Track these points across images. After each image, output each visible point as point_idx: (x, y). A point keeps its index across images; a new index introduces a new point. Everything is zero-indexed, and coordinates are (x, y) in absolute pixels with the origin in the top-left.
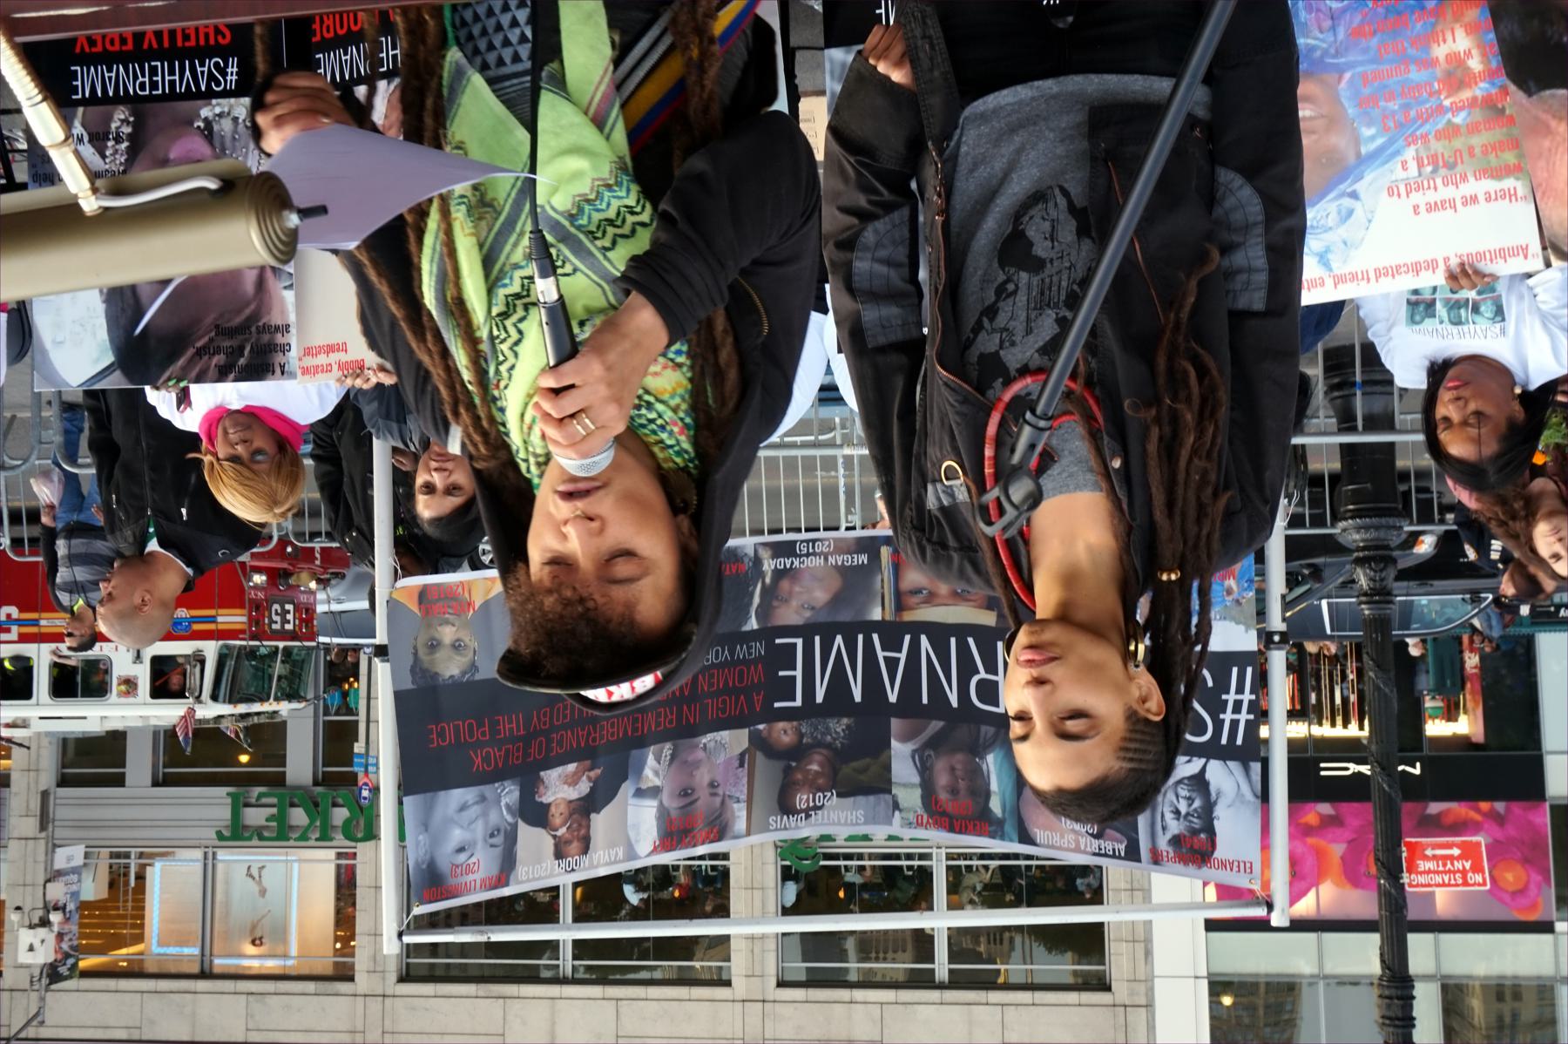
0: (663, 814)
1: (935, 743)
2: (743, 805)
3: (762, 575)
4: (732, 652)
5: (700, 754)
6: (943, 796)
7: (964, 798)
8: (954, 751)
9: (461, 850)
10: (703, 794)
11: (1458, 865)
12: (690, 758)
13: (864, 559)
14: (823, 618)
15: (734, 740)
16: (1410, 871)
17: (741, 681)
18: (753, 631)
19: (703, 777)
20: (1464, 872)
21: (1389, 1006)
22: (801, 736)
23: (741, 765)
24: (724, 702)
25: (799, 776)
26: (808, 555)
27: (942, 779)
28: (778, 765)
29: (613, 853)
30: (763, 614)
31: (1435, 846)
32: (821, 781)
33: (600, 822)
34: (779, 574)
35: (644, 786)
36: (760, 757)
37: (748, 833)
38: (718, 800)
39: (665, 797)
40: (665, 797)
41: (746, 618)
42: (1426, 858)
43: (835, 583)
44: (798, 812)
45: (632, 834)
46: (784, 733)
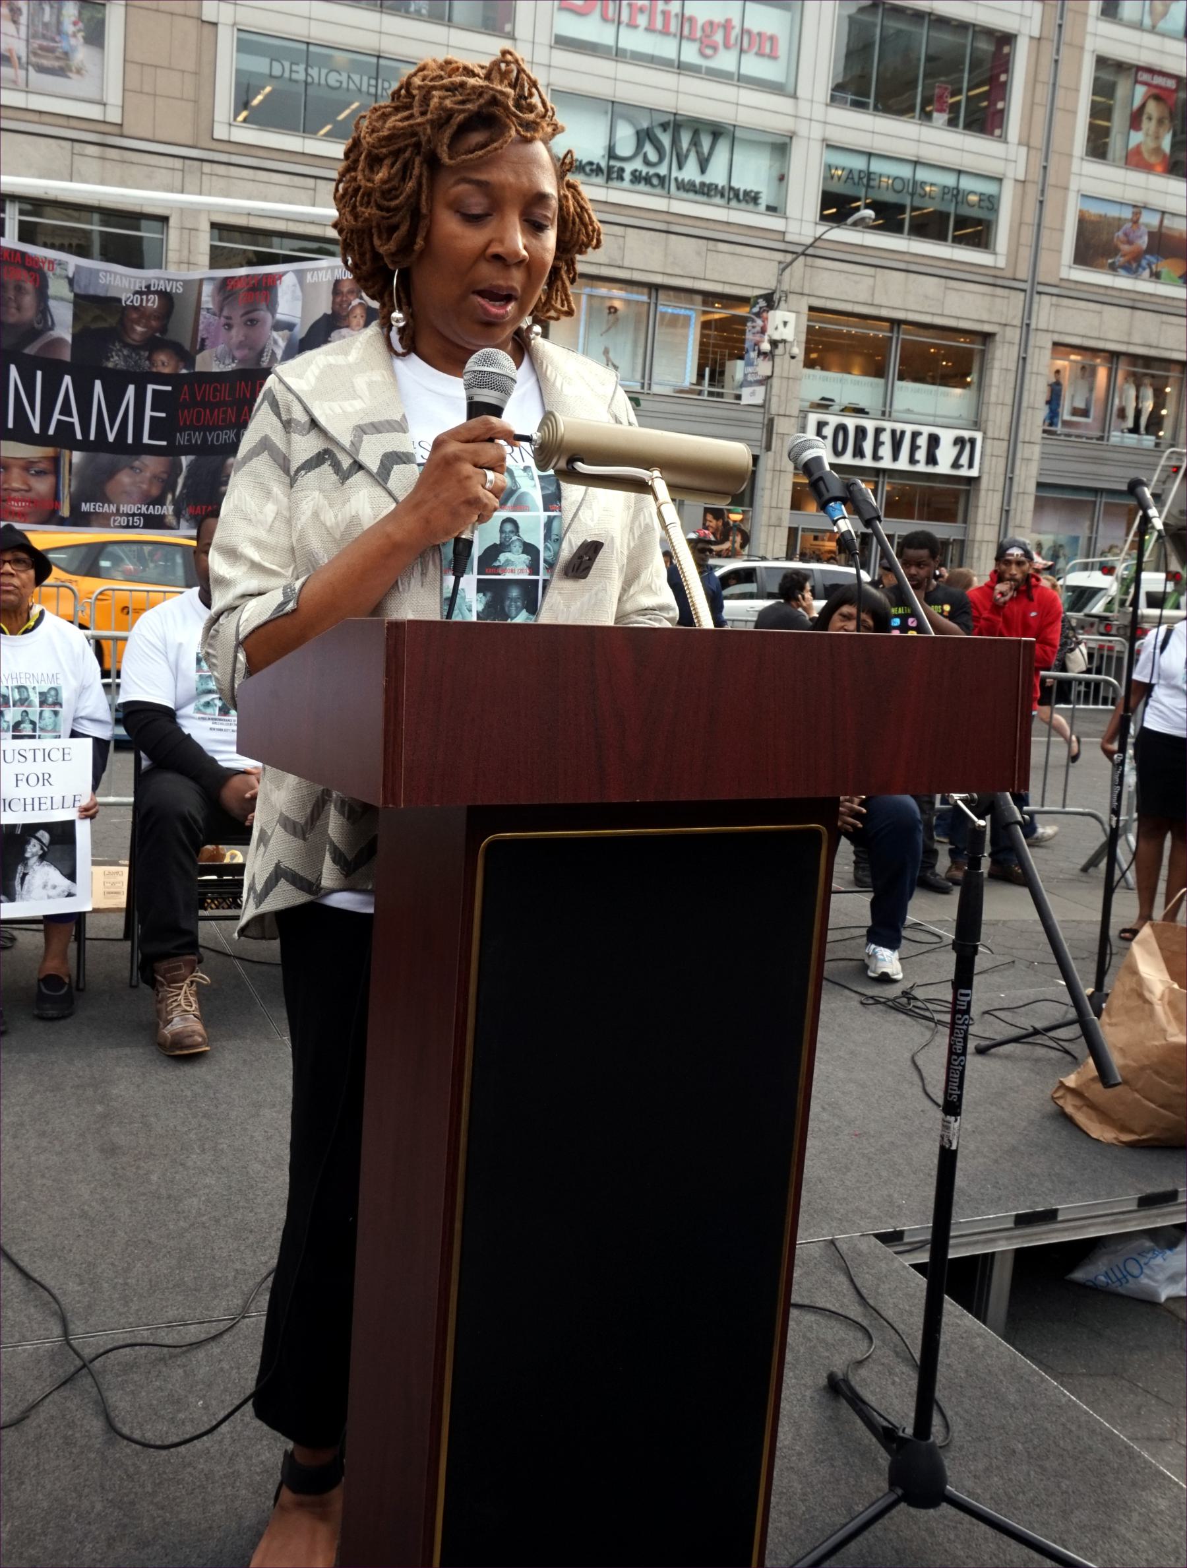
0: (272, 306)
2: (204, 306)
3: (175, 502)
4: (205, 439)
5: (238, 354)
10: (237, 320)
12: (246, 351)
14: (124, 458)
15: (210, 362)
17: (199, 413)
18: (186, 454)
19: (237, 334)
22: (149, 358)
23: (203, 340)
24: (215, 397)
25: (154, 323)
28: (171, 336)
29: (315, 279)
32: (135, 316)
33: (324, 306)
35: (286, 332)
36: (187, 346)
37: (201, 281)
38: (225, 313)
39: (270, 322)
40: (270, 322)
41: (190, 466)
44: (156, 292)
45: (299, 293)
46: (164, 363)
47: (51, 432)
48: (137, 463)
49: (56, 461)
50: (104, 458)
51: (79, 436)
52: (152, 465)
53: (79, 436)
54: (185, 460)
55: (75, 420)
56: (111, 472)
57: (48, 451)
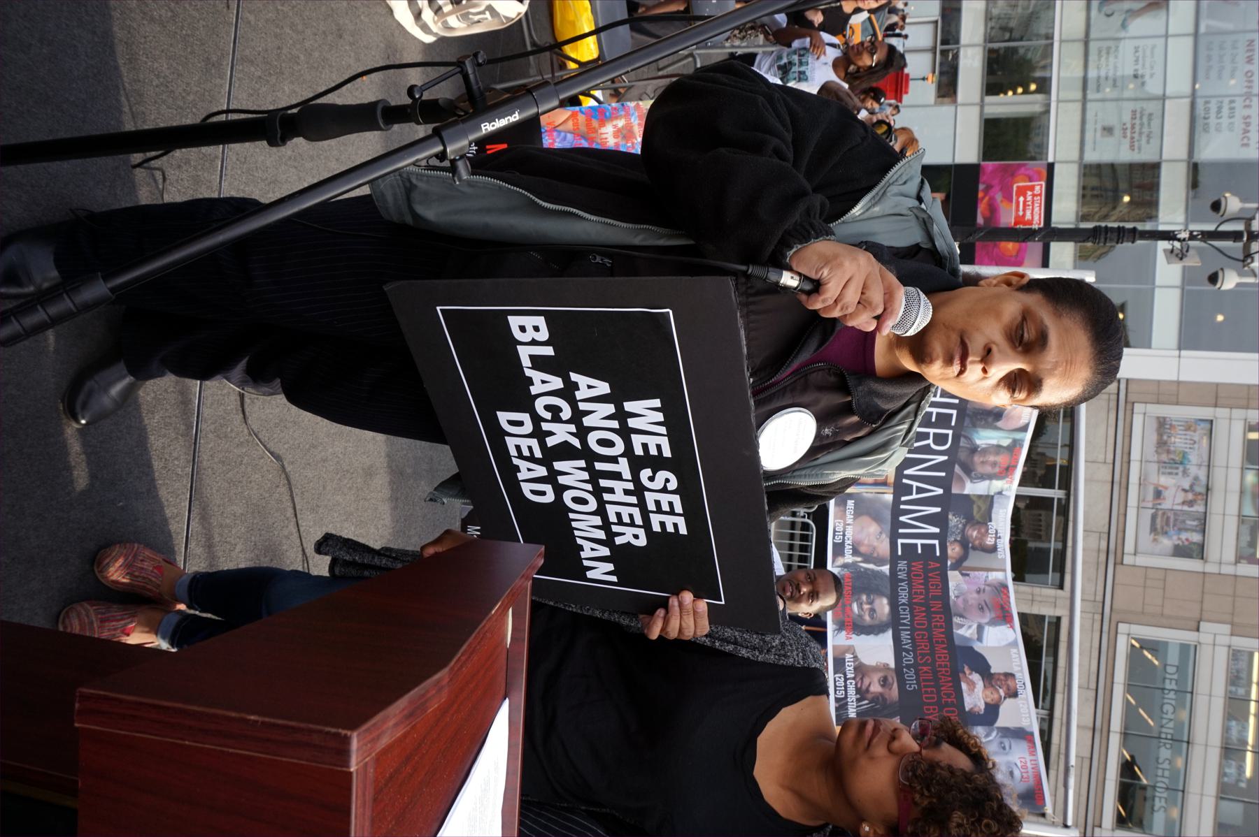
1: (968, 470)
6: (997, 470)
7: (999, 459)
8: (972, 461)
9: (1011, 773)
11: (1029, 198)
13: (850, 503)
16: (1031, 222)
18: (891, 569)
20: (1034, 195)
21: (1111, 240)
26: (844, 535)
27: (988, 469)
30: (880, 562)
31: (1017, 209)
34: (856, 552)
42: (1024, 215)
43: (865, 520)
47: (905, 481)
48: (884, 536)
49: (884, 484)
50: (887, 515)
51: (903, 499)
52: (884, 547)
53: (903, 499)
54: (886, 569)
55: (914, 496)
56: (877, 518)
57: (891, 479)
